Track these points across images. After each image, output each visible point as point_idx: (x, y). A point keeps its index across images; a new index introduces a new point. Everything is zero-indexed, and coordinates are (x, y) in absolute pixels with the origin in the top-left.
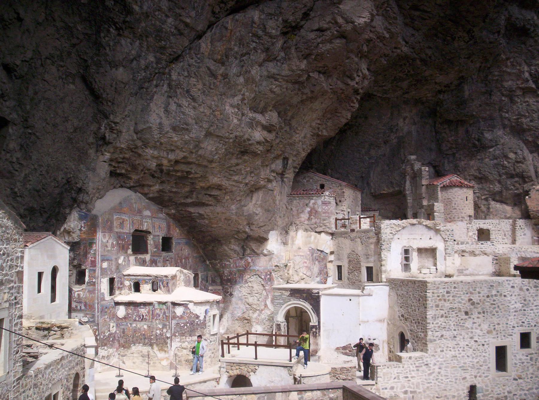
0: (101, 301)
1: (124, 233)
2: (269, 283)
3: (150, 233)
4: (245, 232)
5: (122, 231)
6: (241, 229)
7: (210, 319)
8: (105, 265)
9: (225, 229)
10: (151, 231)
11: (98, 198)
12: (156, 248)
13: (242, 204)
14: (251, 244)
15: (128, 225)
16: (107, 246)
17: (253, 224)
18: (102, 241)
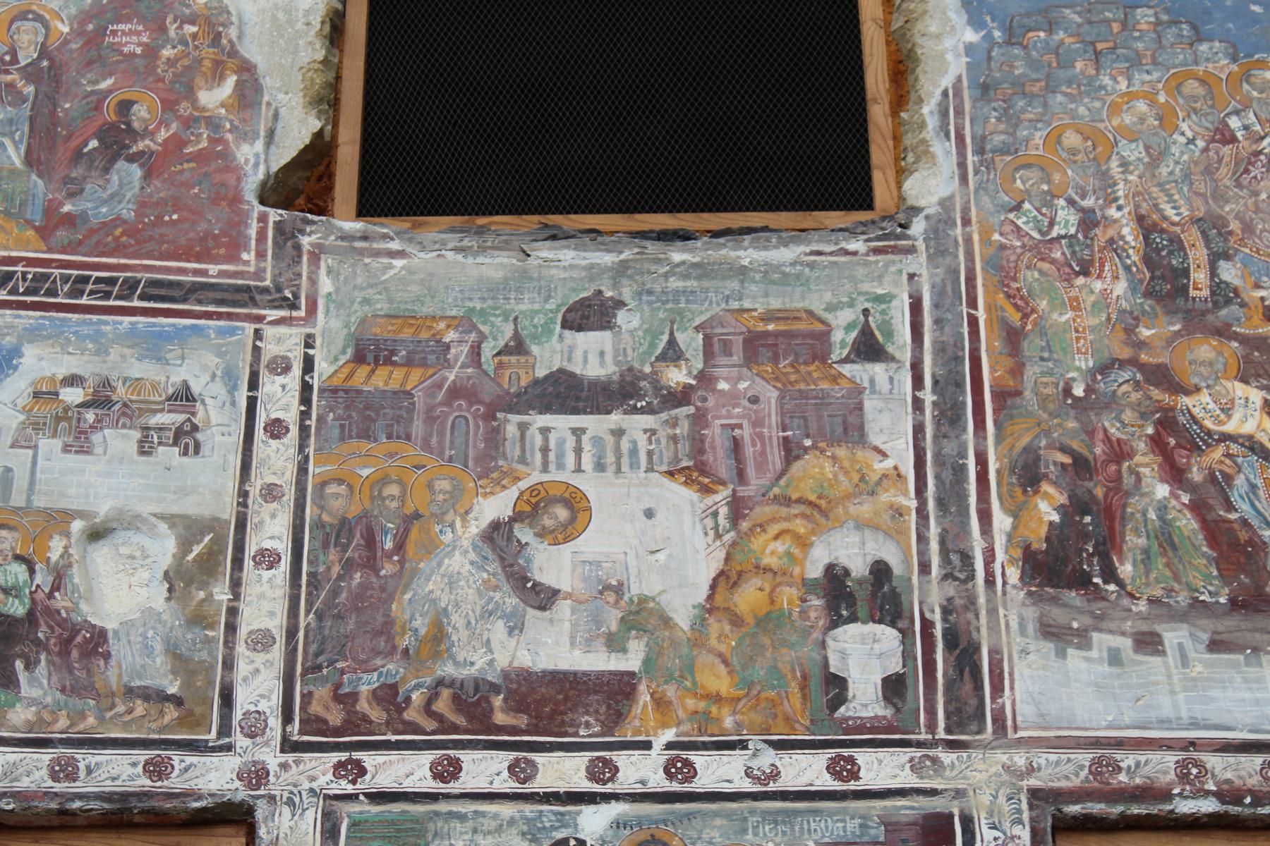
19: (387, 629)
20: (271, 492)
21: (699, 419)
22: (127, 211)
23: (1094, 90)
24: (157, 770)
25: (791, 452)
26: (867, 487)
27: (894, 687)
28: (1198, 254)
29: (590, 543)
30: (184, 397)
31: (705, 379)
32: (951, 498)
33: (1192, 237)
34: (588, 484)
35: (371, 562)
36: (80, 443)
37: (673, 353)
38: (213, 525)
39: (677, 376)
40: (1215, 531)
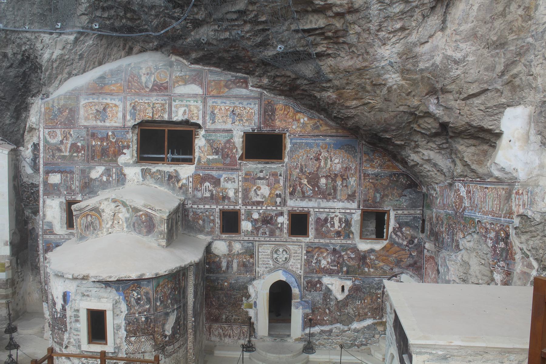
0: (45, 232)
1: (109, 128)
2: (502, 264)
3: (198, 126)
4: (428, 114)
5: (99, 123)
6: (417, 108)
7: (77, 316)
8: (55, 179)
9: (381, 110)
10: (200, 122)
11: (70, 75)
12: (217, 153)
13: (413, 38)
14: (461, 148)
15: (120, 115)
16: (60, 150)
17: (444, 91)
18: (46, 141)
19: (248, 197)
20: (240, 186)
21: (269, 181)
22: (229, 162)
23: (299, 151)
24: (234, 207)
25: (275, 184)
26: (280, 187)
27: (280, 203)
28: (304, 168)
29: (261, 191)
30: (234, 178)
31: (269, 177)
32: (285, 188)
33: (304, 166)
34: (261, 186)
35: (247, 192)
36: (227, 183)
37: (267, 175)
38: (237, 189)
39: (267, 177)
40: (302, 191)
